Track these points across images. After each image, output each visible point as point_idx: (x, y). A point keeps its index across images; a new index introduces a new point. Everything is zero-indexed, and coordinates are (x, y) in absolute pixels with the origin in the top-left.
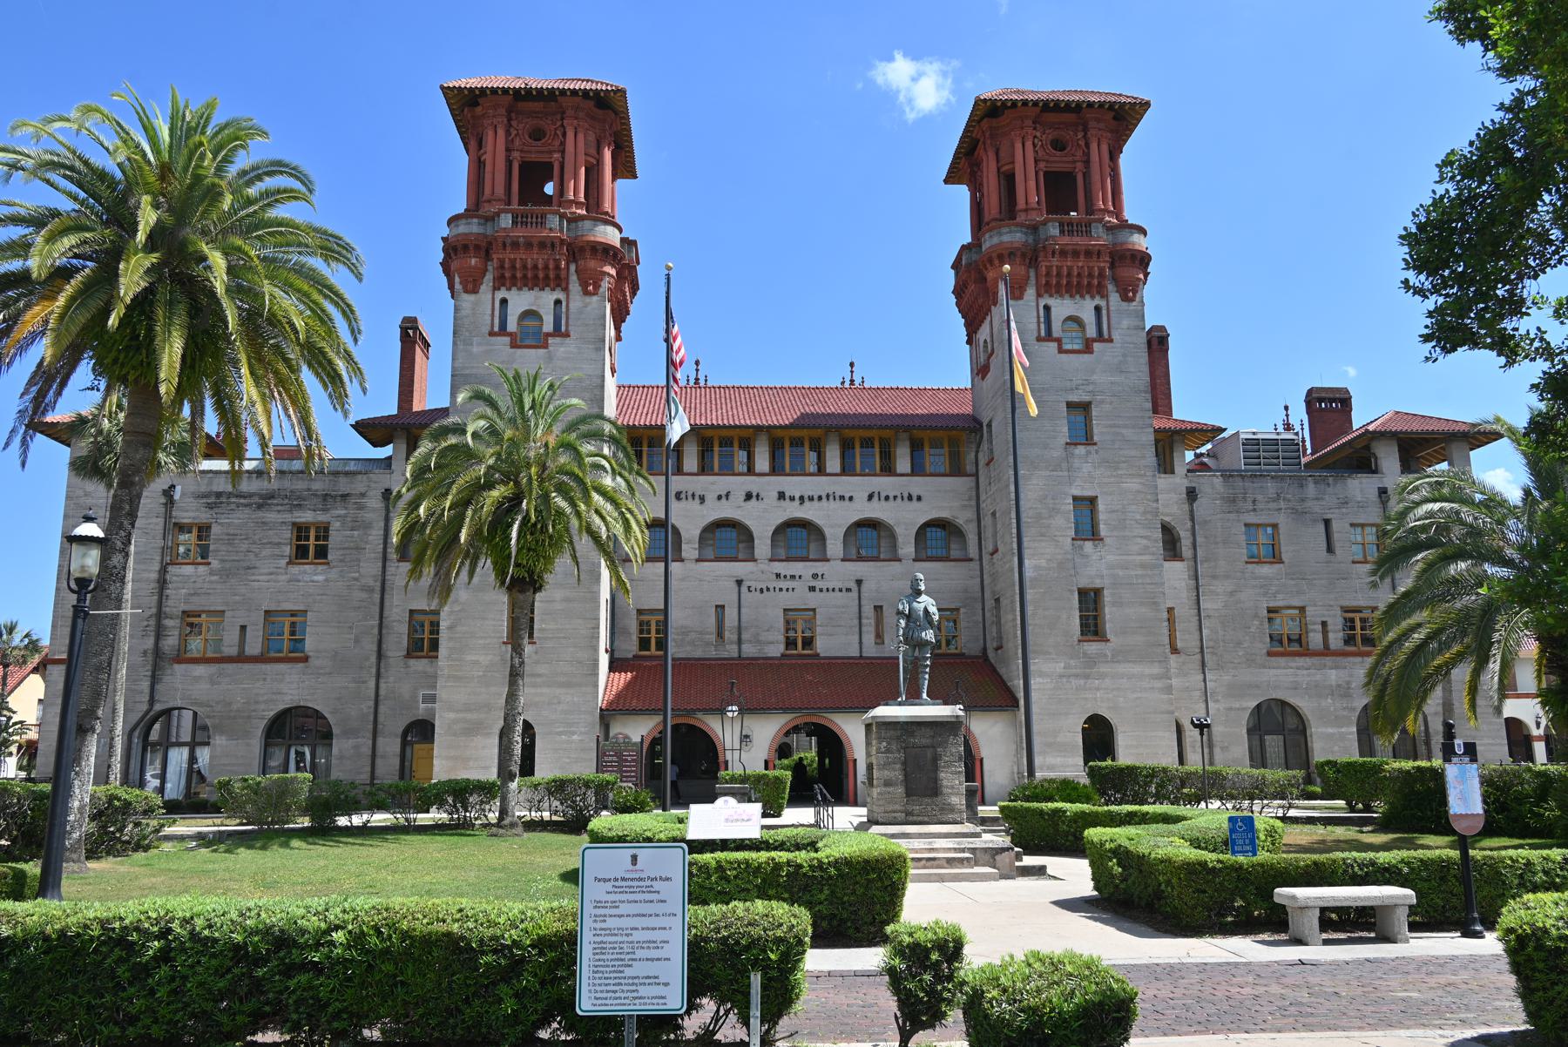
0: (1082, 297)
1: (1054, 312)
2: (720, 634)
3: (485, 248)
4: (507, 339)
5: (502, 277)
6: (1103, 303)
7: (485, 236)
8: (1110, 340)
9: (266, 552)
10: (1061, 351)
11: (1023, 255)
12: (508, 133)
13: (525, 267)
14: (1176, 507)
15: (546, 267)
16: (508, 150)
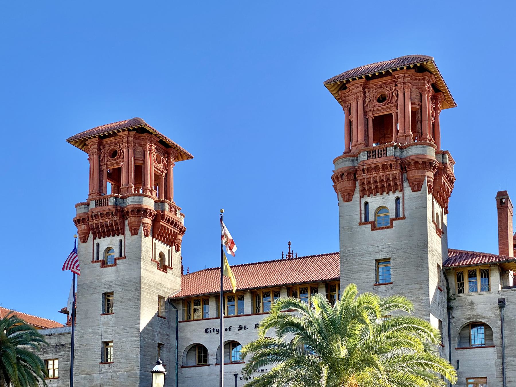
0: (388, 193)
4: (99, 264)
6: (400, 195)
8: (404, 218)
12: (99, 157)
14: (490, 312)
16: (100, 166)
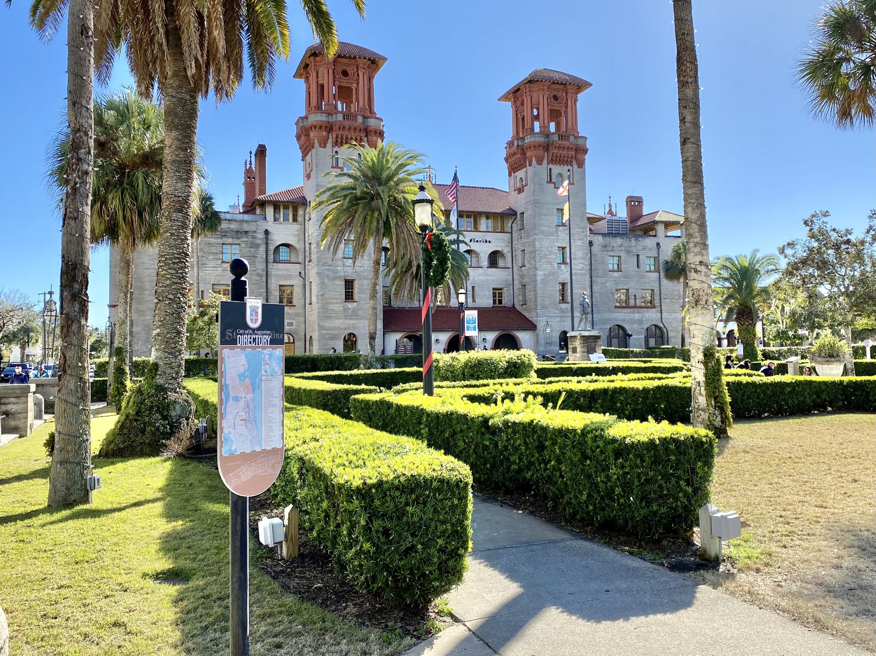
1: (553, 171)
5: (337, 141)
7: (329, 122)
9: (211, 257)
12: (334, 73)
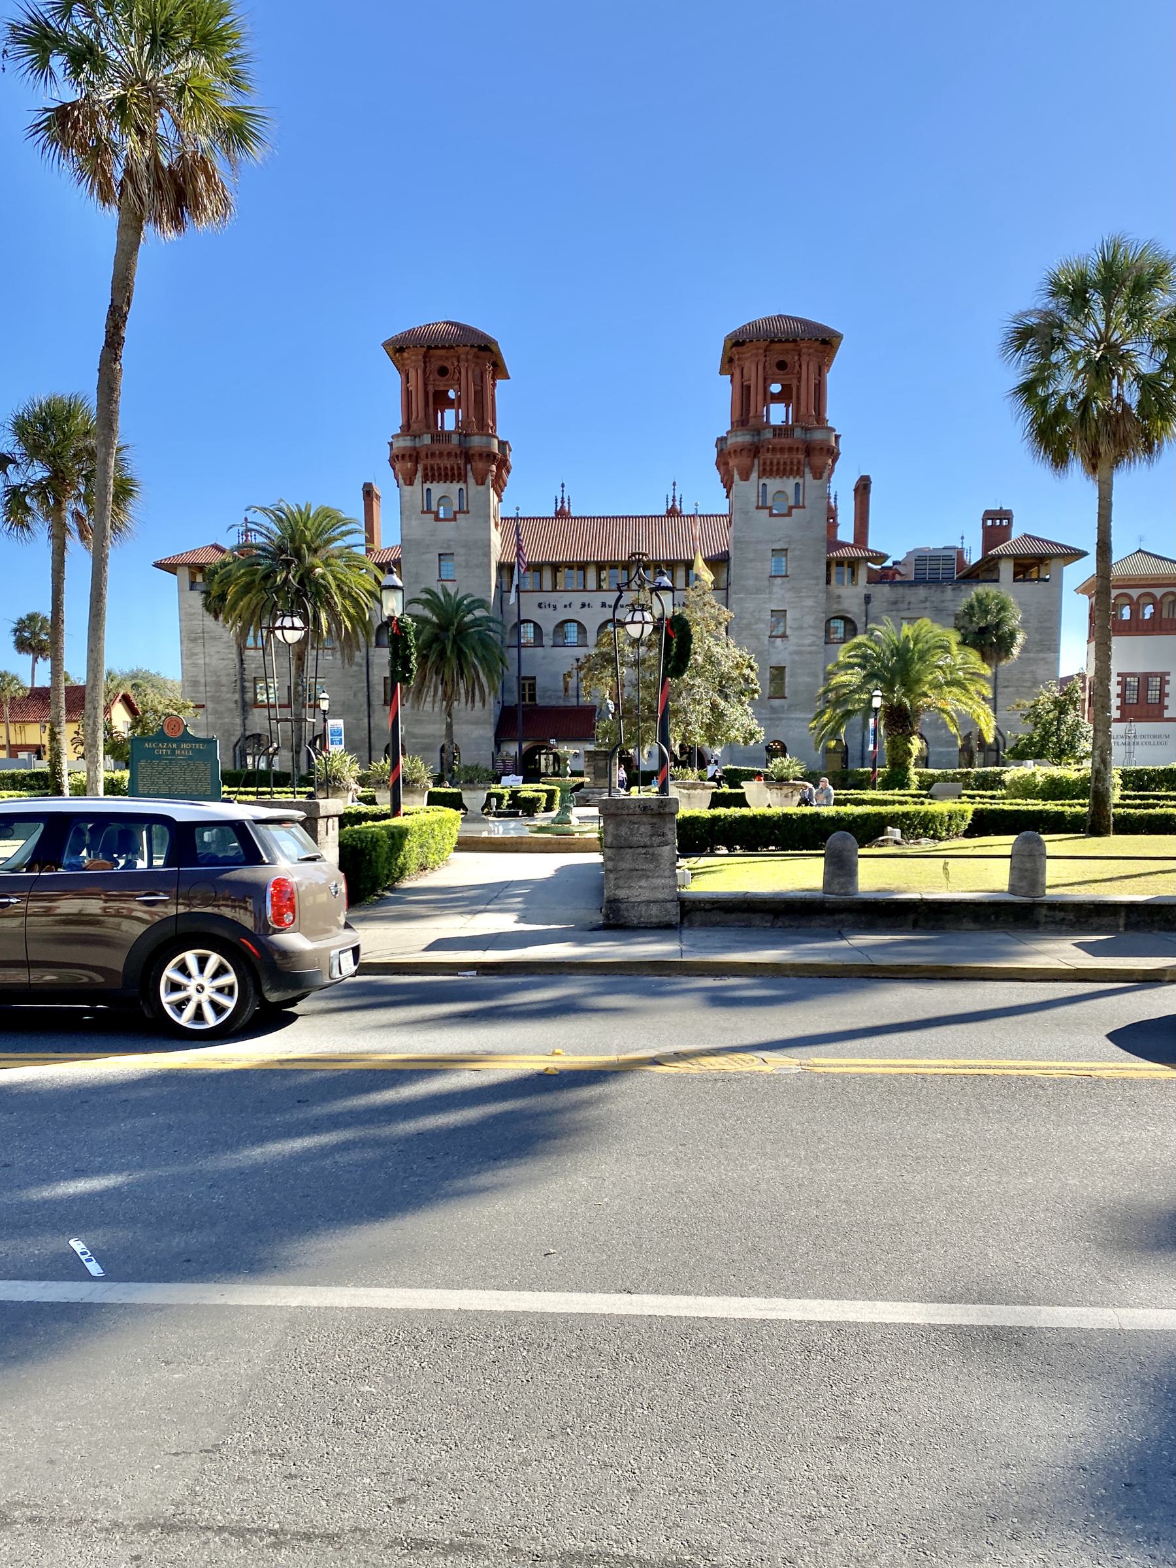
0: (788, 477)
1: (769, 489)
2: (566, 690)
3: (413, 456)
4: (432, 516)
6: (800, 481)
7: (415, 448)
8: (803, 507)
10: (771, 515)
11: (750, 450)
13: (440, 468)
15: (452, 468)
